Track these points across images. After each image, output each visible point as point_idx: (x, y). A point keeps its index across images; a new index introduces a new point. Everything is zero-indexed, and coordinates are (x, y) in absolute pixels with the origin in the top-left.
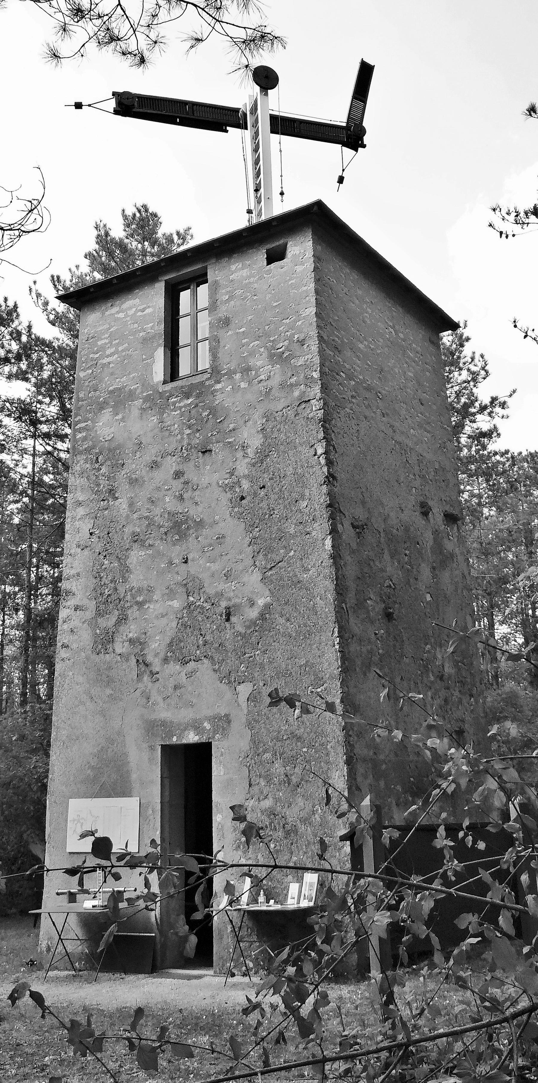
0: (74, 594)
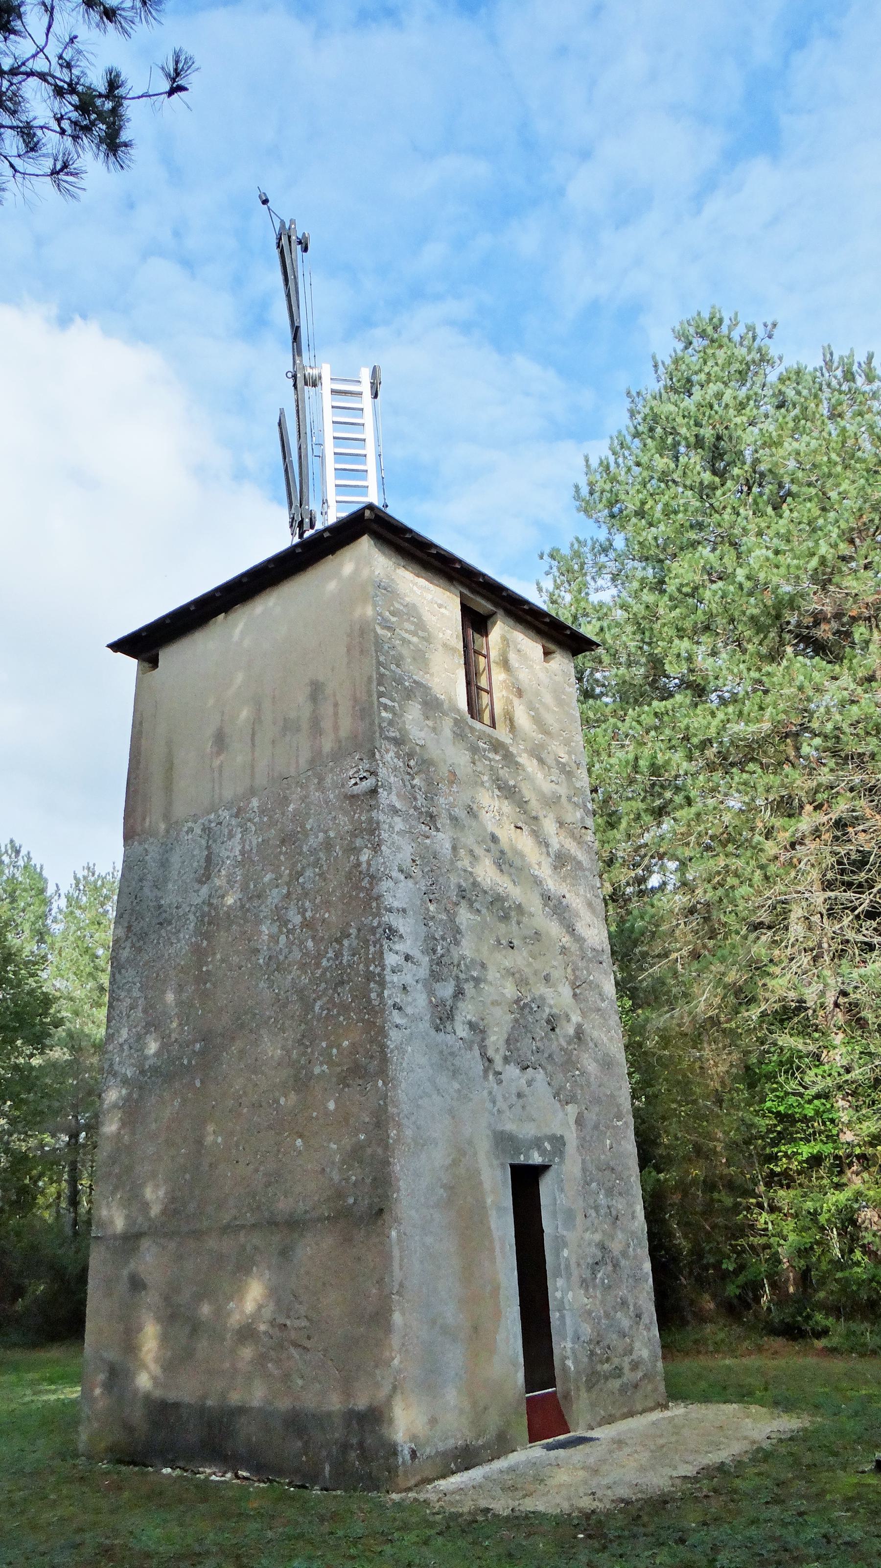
0: (401, 937)
